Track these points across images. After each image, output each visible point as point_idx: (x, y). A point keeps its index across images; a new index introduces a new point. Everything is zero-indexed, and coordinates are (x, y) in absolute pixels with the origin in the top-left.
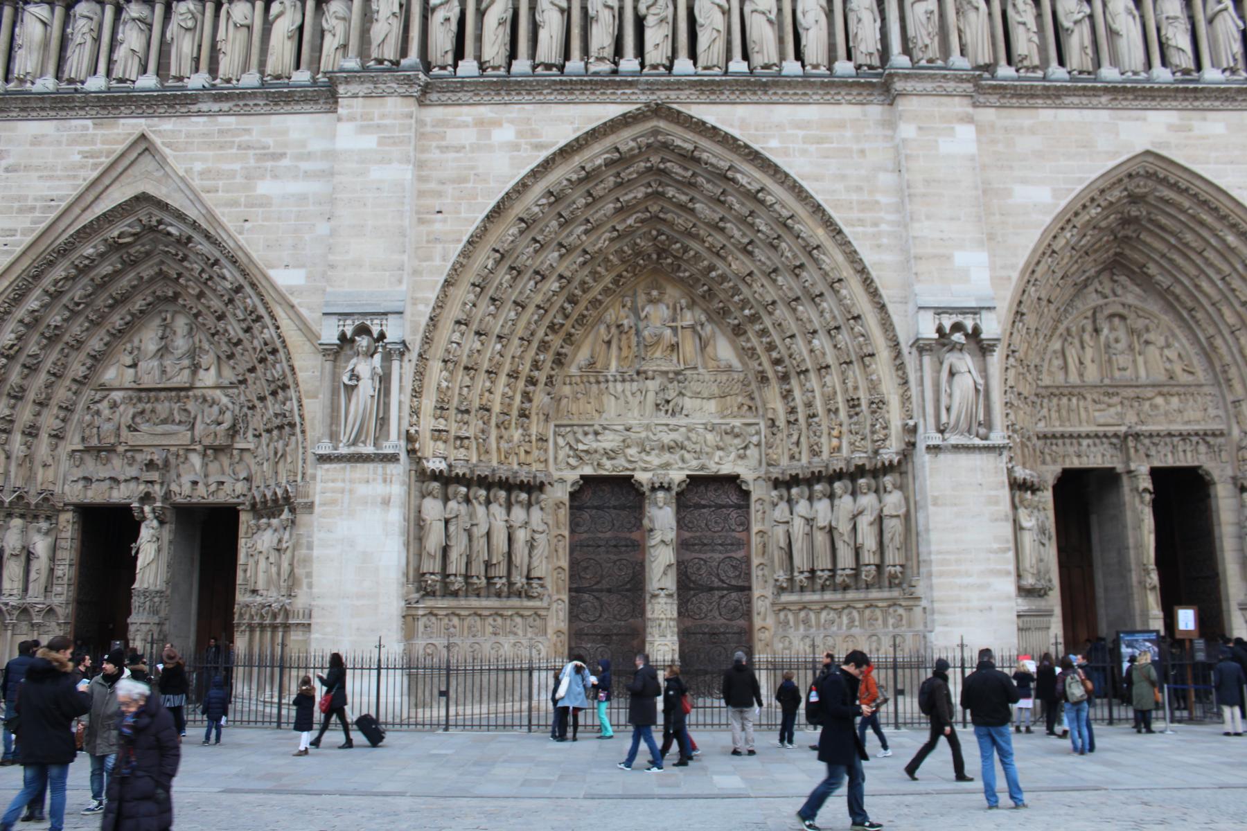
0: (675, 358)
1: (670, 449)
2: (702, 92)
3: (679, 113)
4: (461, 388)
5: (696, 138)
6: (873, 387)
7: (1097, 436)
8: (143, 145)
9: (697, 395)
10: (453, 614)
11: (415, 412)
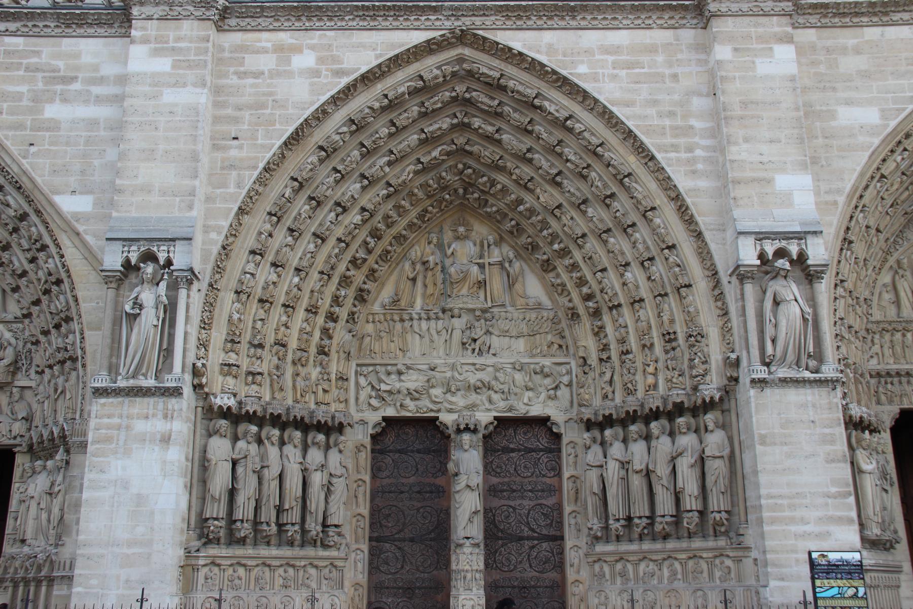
1: (476, 389)
2: (508, 17)
3: (485, 39)
4: (254, 321)
5: (502, 65)
6: (691, 319)
9: (505, 334)
10: (239, 564)
11: (203, 345)
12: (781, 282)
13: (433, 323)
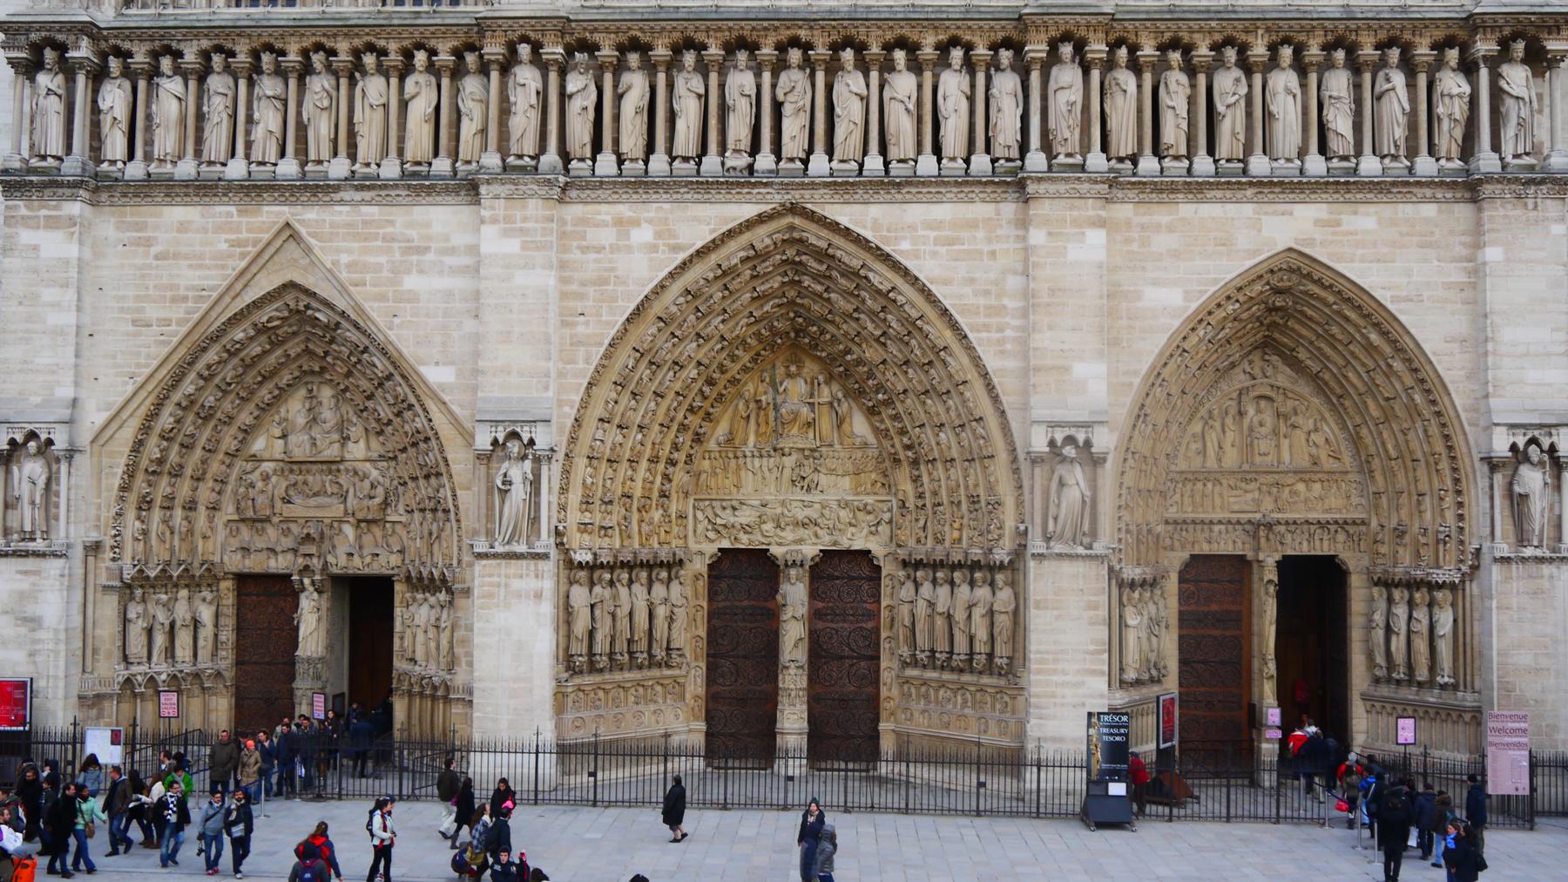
0: (811, 435)
6: (991, 489)
7: (1229, 522)
8: (289, 232)
9: (832, 471)
11: (563, 508)
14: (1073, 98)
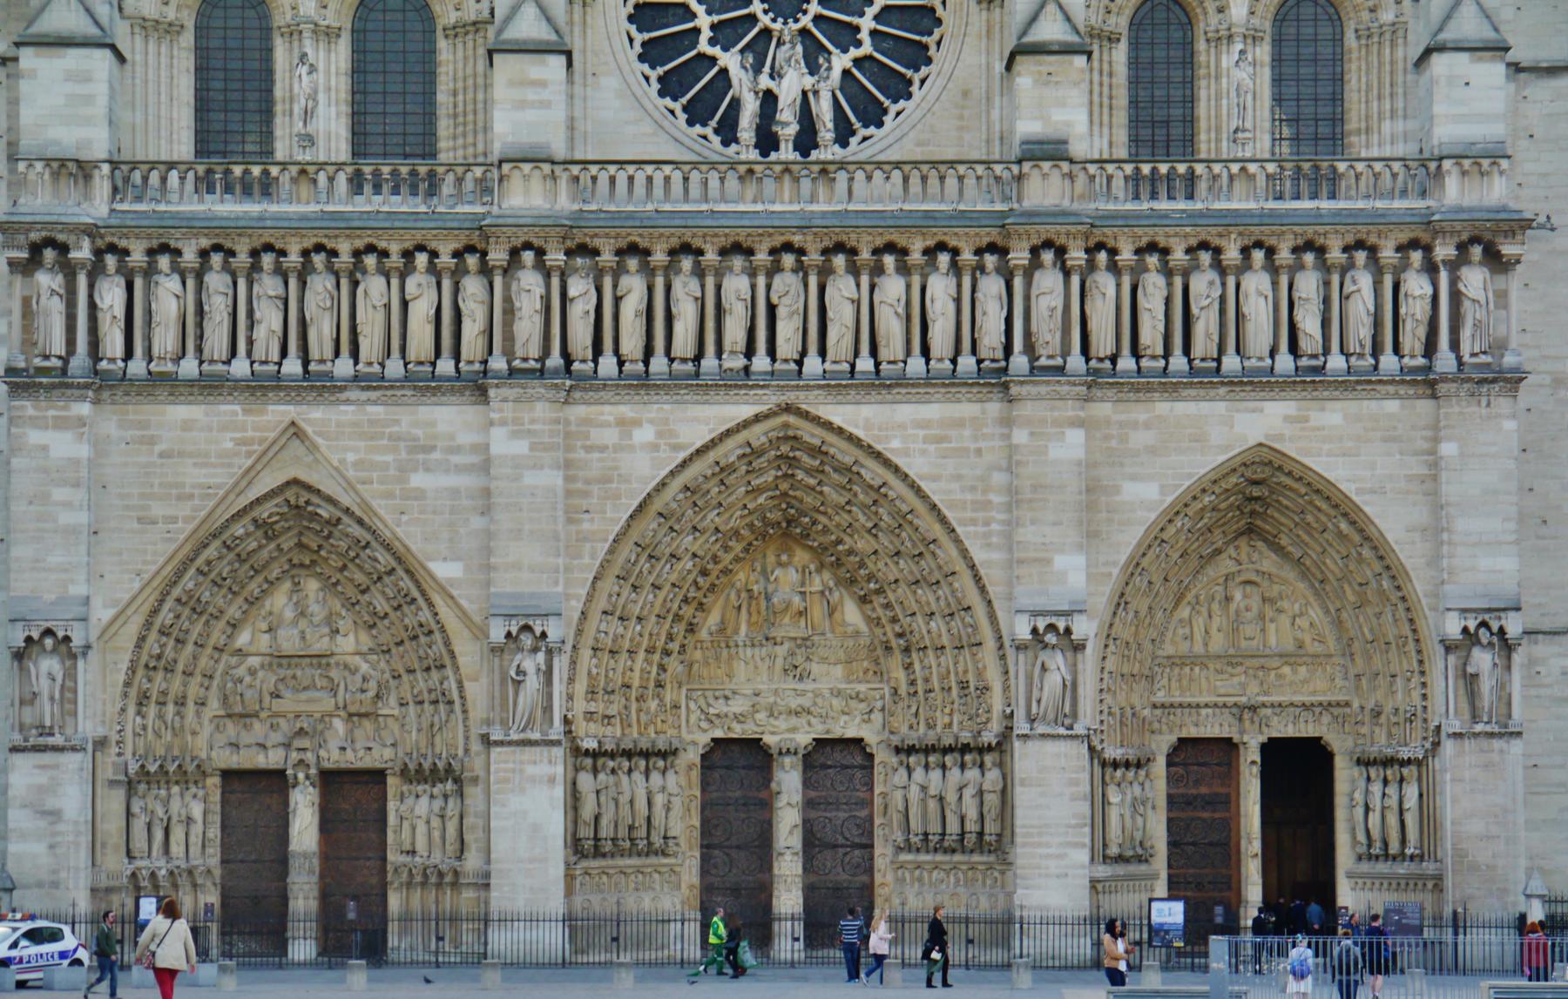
6: (980, 674)
7: (1216, 705)
9: (824, 660)
11: (570, 697)
12: (1048, 652)
13: (757, 650)
14: (1053, 304)
